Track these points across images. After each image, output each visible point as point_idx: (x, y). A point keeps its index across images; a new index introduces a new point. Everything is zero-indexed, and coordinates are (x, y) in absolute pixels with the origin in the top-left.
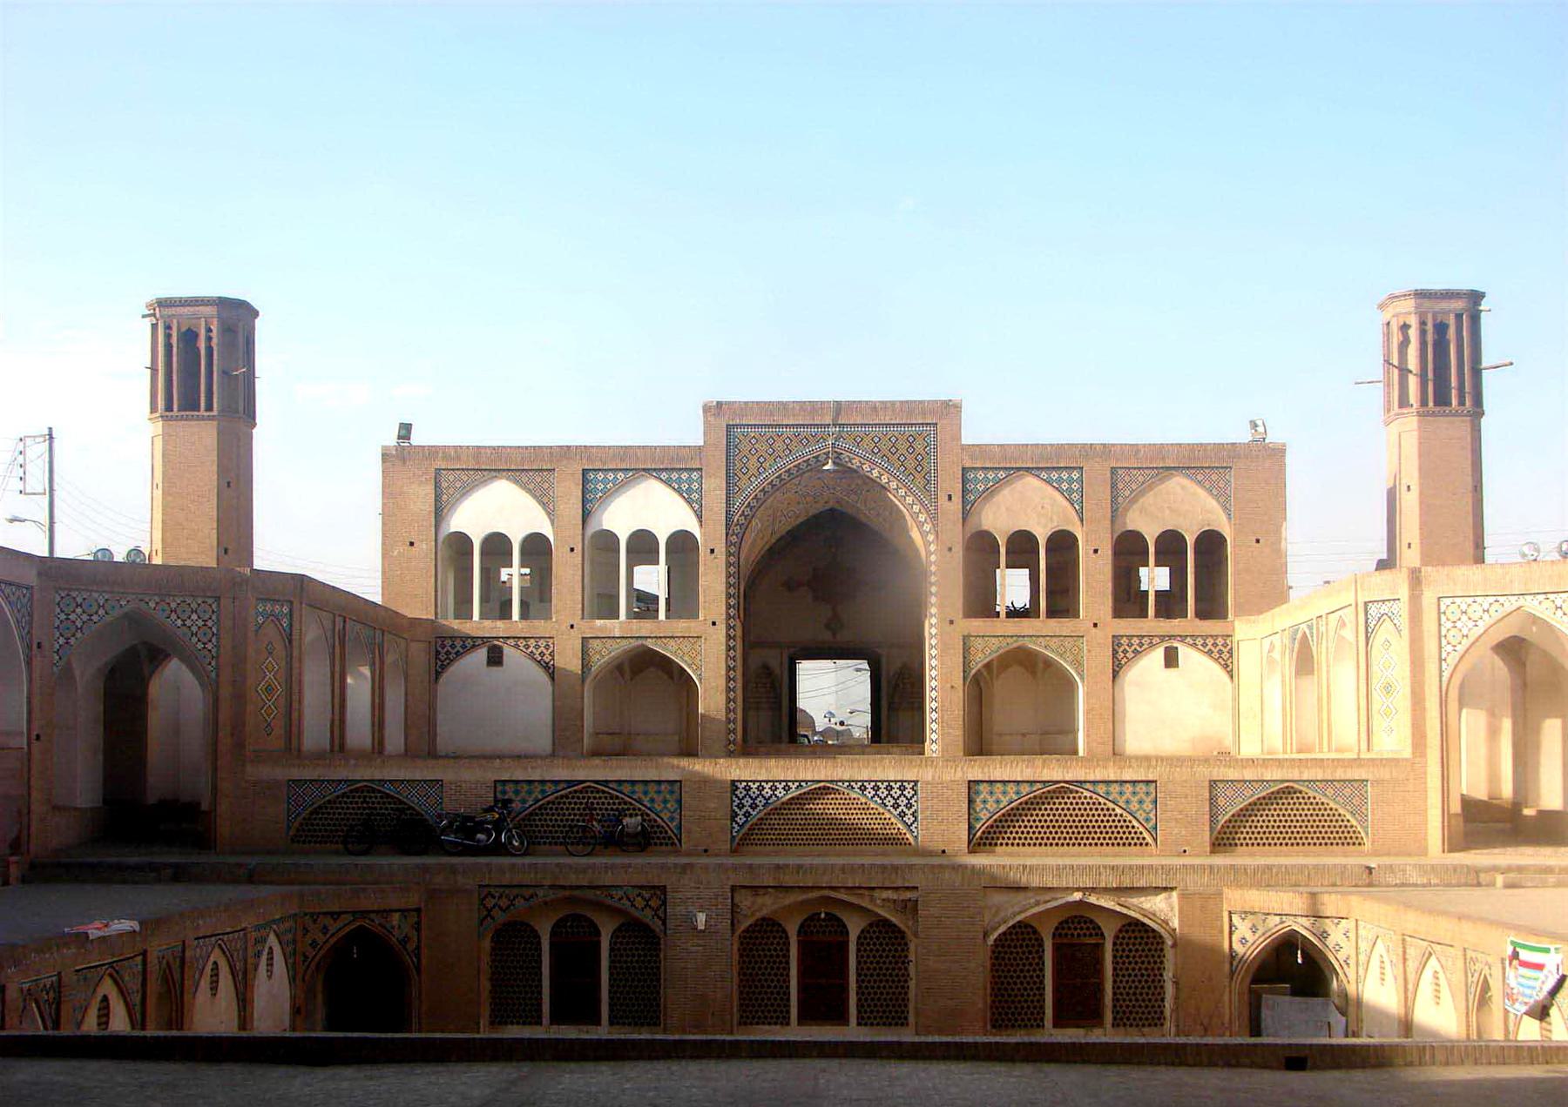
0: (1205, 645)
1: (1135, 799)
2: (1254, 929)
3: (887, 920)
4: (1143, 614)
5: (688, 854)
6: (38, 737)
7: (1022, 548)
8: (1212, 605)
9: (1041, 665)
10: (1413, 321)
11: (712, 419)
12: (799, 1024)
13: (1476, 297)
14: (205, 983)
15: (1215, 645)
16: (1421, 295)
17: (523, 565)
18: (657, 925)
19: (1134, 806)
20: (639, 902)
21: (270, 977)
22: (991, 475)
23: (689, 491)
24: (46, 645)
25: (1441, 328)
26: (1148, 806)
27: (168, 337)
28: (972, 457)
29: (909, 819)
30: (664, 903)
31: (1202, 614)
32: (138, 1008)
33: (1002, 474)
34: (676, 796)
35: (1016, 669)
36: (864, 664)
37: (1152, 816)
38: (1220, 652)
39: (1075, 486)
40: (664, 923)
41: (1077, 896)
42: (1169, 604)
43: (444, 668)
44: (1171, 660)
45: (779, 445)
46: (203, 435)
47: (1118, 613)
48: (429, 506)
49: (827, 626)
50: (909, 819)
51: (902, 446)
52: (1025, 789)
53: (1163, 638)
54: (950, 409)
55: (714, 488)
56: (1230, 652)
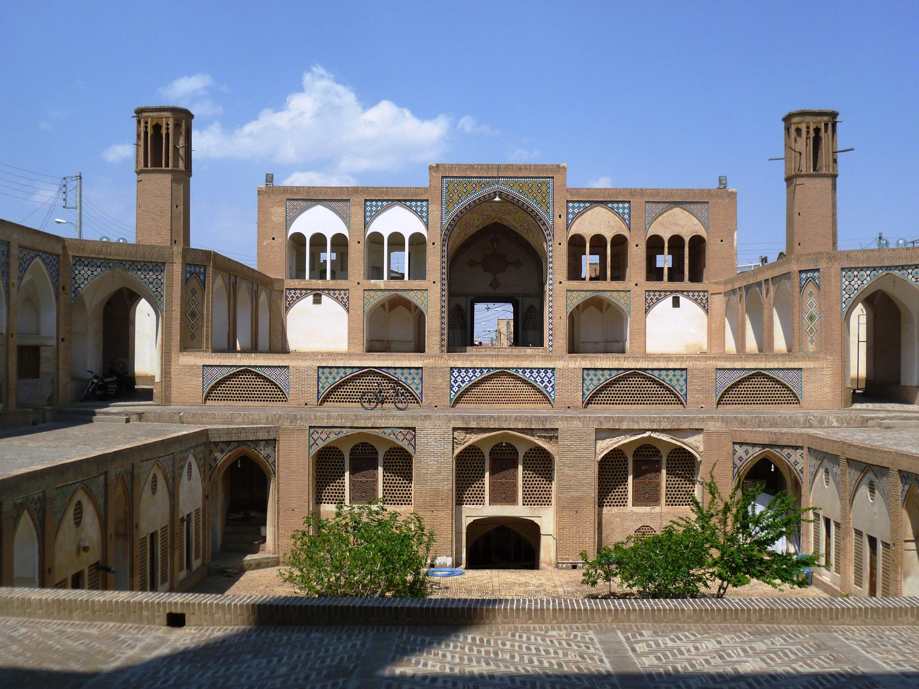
0: (693, 296)
1: (674, 379)
2: (747, 452)
3: (540, 447)
4: (660, 279)
6: (63, 340)
7: (598, 242)
8: (696, 276)
9: (605, 307)
10: (803, 127)
13: (834, 115)
14: (148, 488)
15: (699, 296)
17: (332, 251)
18: (410, 449)
19: (674, 383)
21: (189, 479)
22: (582, 205)
23: (422, 211)
24: (67, 288)
25: (817, 130)
26: (682, 382)
27: (146, 127)
28: (572, 195)
29: (550, 389)
31: (692, 280)
32: (102, 507)
33: (587, 205)
34: (420, 376)
35: (592, 308)
36: (509, 307)
37: (684, 388)
38: (702, 299)
39: (626, 211)
40: (414, 448)
41: (647, 434)
42: (675, 274)
44: (676, 303)
46: (162, 182)
47: (649, 279)
48: (282, 220)
49: (491, 285)
50: (550, 389)
51: (535, 189)
52: (614, 373)
53: (671, 292)
55: (435, 211)
56: (707, 299)
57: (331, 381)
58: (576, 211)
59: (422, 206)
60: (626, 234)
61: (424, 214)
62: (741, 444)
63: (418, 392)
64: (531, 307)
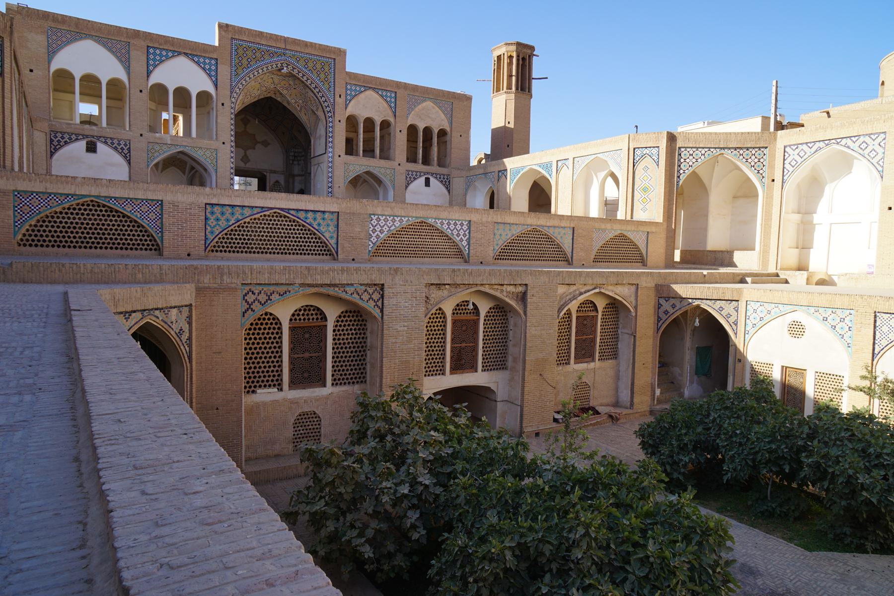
2: (674, 306)
5: (345, 261)
10: (514, 54)
11: (223, 33)
12: (451, 373)
16: (519, 44)
20: (366, 297)
22: (358, 89)
28: (350, 78)
30: (382, 297)
39: (393, 100)
40: (382, 311)
43: (56, 150)
44: (427, 183)
45: (258, 55)
47: (408, 160)
50: (465, 243)
51: (319, 66)
54: (341, 53)
55: (224, 71)
57: (223, 223)
58: (353, 93)
59: (210, 64)
60: (392, 120)
61: (213, 73)
62: (667, 299)
63: (333, 242)
64: (277, 182)
